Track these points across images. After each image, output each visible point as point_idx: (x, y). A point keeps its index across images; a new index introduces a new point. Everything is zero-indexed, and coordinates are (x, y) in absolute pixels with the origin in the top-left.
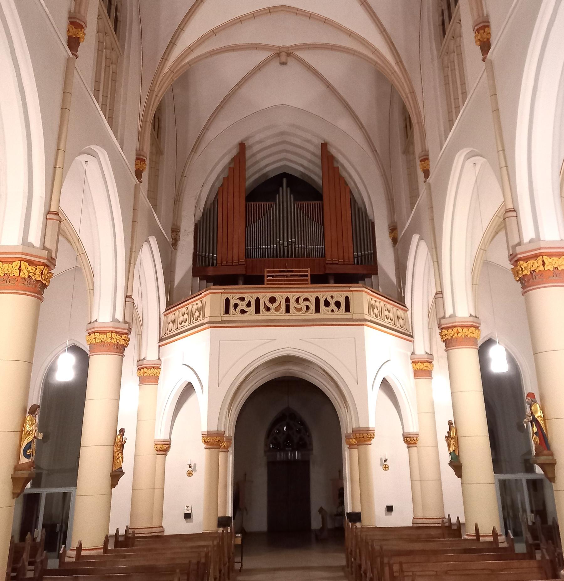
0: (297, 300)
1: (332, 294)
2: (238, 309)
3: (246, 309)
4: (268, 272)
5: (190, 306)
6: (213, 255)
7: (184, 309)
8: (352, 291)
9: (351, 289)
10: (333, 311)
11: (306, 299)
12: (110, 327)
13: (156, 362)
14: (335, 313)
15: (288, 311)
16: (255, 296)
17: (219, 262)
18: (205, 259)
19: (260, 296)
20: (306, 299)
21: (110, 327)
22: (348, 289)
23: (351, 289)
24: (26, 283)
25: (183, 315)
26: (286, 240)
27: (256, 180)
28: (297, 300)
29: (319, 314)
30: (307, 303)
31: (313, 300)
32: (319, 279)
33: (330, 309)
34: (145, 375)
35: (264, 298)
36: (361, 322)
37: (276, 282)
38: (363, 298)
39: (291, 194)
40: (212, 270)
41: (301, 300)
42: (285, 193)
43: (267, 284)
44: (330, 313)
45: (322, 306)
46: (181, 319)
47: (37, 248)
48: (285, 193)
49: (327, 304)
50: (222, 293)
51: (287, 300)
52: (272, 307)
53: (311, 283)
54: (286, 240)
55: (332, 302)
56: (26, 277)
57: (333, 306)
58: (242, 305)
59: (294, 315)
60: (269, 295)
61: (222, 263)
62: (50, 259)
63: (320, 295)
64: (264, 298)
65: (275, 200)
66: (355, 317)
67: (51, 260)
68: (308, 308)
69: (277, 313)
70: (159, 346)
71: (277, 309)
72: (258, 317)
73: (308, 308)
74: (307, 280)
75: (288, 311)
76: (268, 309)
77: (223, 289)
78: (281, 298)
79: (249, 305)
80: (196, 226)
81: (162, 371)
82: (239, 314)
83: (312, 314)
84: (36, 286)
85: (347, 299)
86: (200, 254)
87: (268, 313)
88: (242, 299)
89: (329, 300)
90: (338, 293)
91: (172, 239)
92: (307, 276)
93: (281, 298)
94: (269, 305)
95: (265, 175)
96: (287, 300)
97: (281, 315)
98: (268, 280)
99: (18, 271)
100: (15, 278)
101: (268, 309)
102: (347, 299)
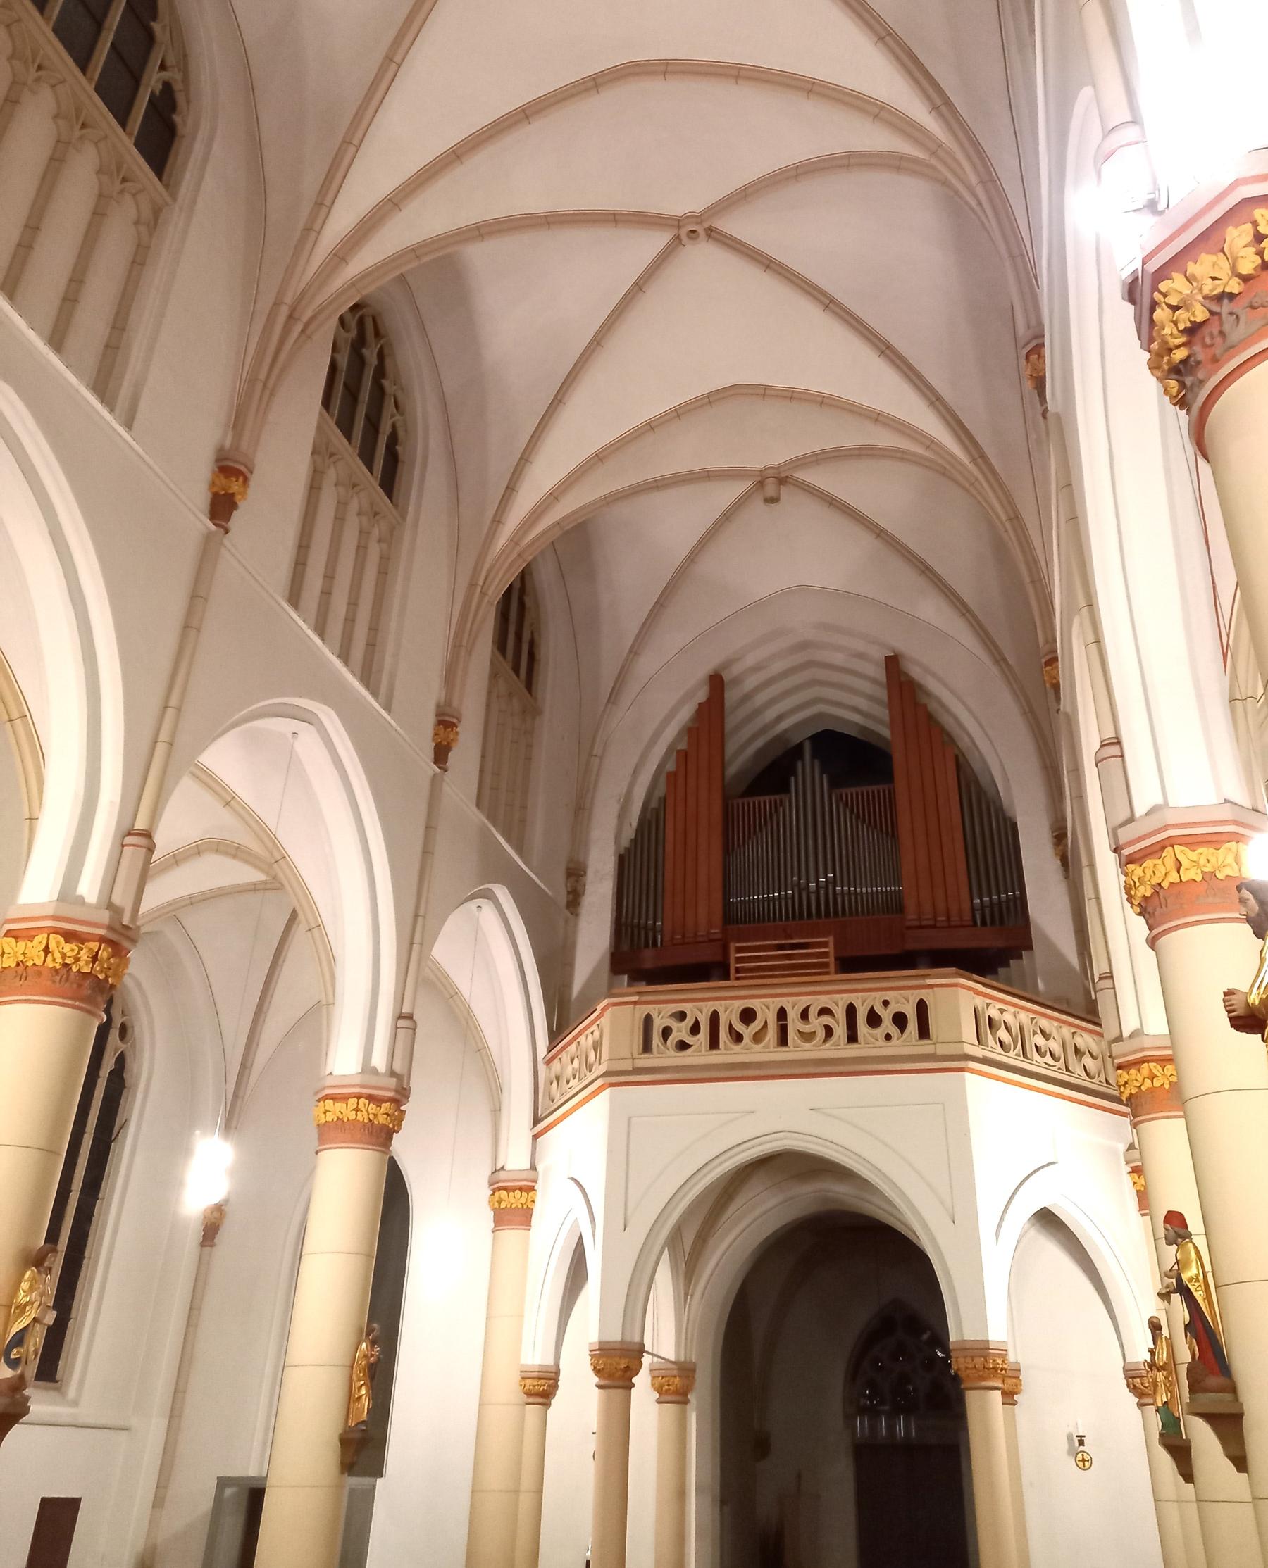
0: (804, 1015)
1: (889, 995)
2: (672, 1039)
3: (689, 1040)
4: (739, 950)
5: (582, 1039)
6: (655, 922)
7: (573, 1047)
8: (931, 986)
9: (929, 982)
10: (888, 1037)
11: (825, 1011)
12: (354, 1086)
13: (524, 1176)
14: (894, 1041)
15: (783, 1040)
16: (708, 1008)
17: (667, 938)
18: (646, 935)
19: (719, 1006)
20: (825, 1011)
21: (354, 1086)
22: (921, 982)
23: (929, 982)
24: (58, 978)
25: (572, 1061)
26: (812, 877)
27: (760, 753)
28: (804, 1015)
29: (855, 1045)
30: (826, 1020)
31: (841, 1013)
32: (851, 964)
33: (880, 1032)
34: (503, 1205)
35: (729, 1011)
36: (956, 1062)
37: (765, 973)
38: (960, 1000)
39: (822, 773)
40: (646, 957)
41: (812, 1014)
42: (809, 772)
43: (738, 979)
44: (882, 1042)
45: (863, 1028)
46: (569, 1071)
47: (90, 906)
48: (809, 772)
49: (874, 1020)
50: (635, 1003)
51: (782, 1014)
52: (748, 1032)
53: (836, 973)
54: (812, 877)
55: (886, 1015)
56: (58, 966)
57: (888, 1025)
58: (680, 1031)
59: (797, 1050)
60: (740, 1005)
61: (672, 938)
62: (118, 927)
63: (856, 999)
64: (729, 1011)
65: (787, 791)
66: (942, 1050)
67: (124, 931)
68: (829, 1031)
69: (757, 1047)
70: (535, 1137)
71: (757, 1038)
72: (716, 1058)
73: (829, 1031)
74: (826, 965)
75: (783, 1040)
76: (738, 1038)
77: (639, 993)
78: (766, 1009)
79: (695, 1029)
80: (622, 861)
81: (539, 1197)
82: (672, 1052)
83: (839, 1048)
84: (79, 986)
85: (922, 1007)
86: (643, 921)
87: (737, 1048)
88: (682, 1016)
89: (879, 1010)
90: (895, 993)
91: (569, 893)
92: (825, 955)
93: (766, 1009)
94: (739, 1027)
95: (779, 738)
96: (782, 1014)
97: (768, 1051)
98: (738, 970)
99: (42, 954)
100: (38, 970)
101: (738, 1038)
102: (922, 1007)
